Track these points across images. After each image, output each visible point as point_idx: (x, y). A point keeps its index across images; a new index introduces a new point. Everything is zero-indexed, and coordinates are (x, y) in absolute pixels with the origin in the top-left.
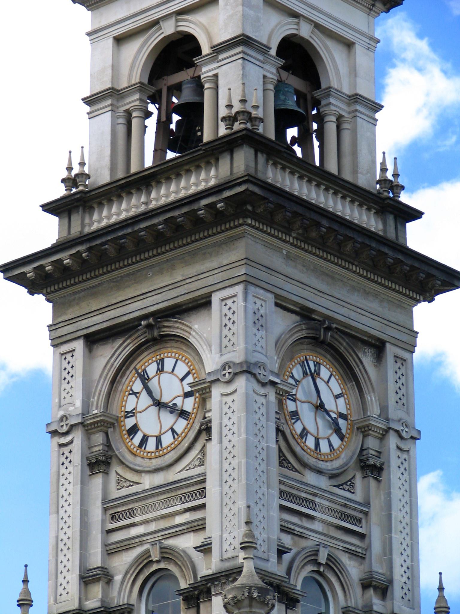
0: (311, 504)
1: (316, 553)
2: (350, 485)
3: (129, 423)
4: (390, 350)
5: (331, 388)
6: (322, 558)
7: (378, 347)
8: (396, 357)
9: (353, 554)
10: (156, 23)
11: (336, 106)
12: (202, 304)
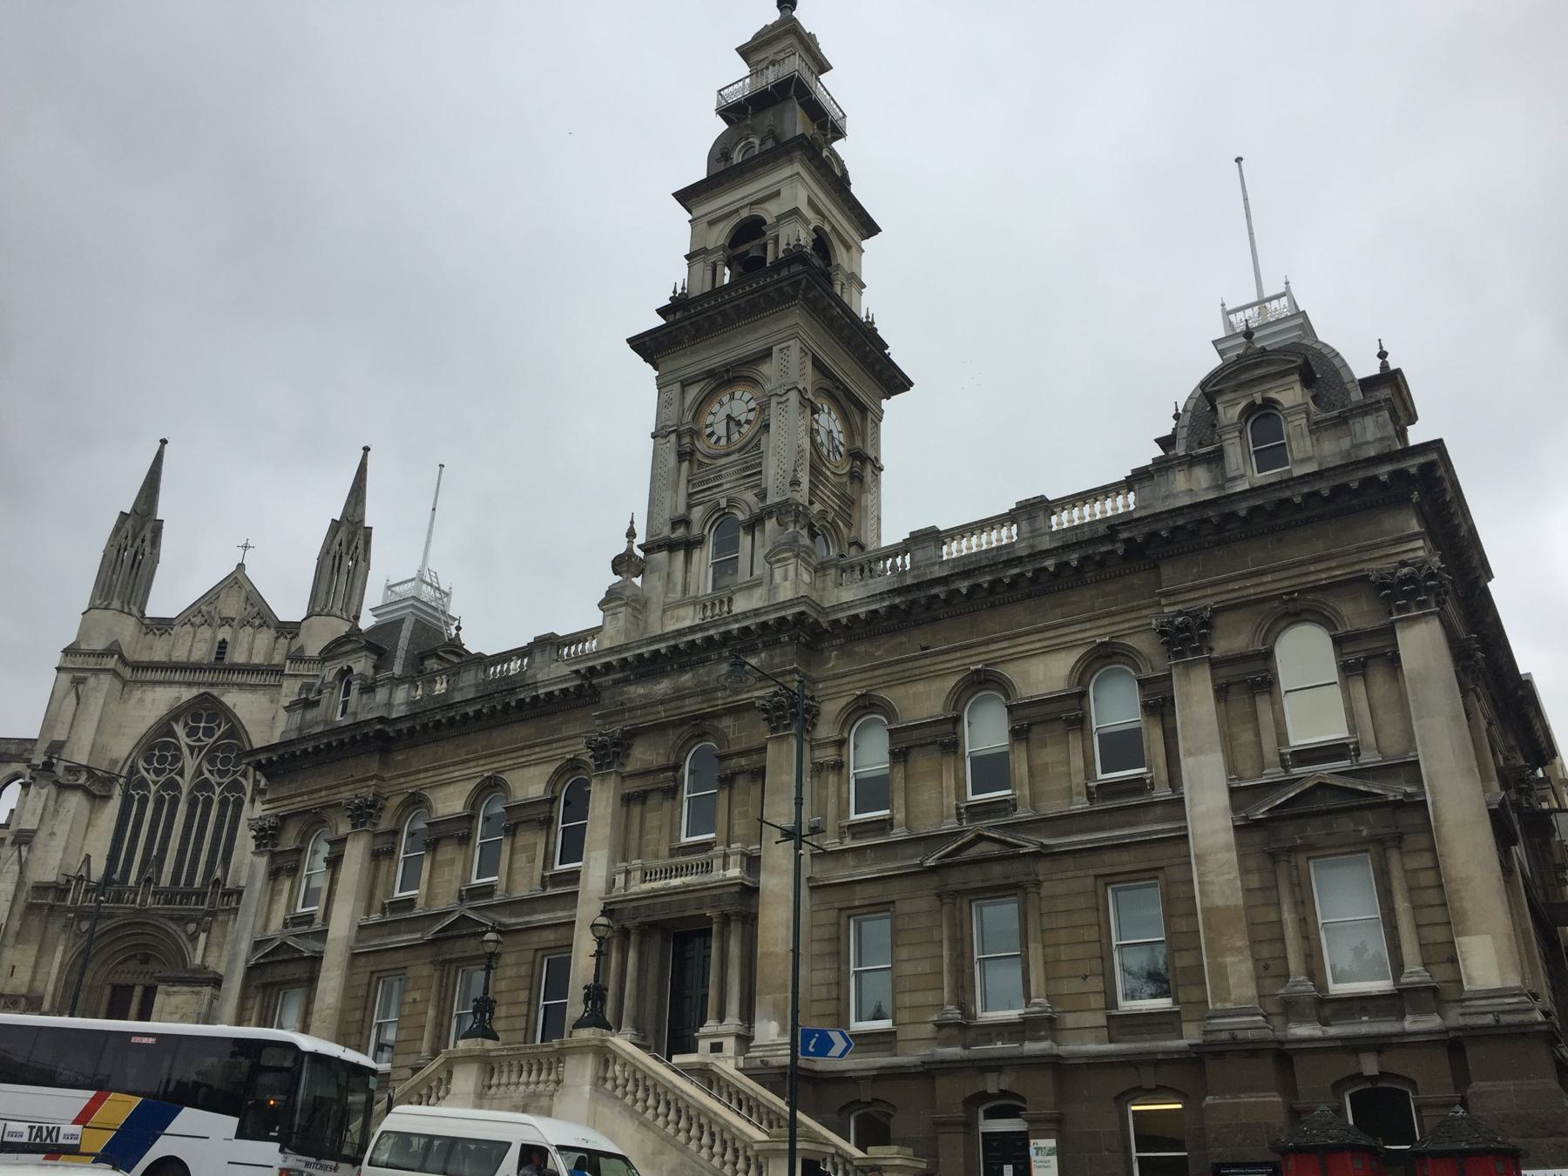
3: (709, 431)
10: (737, 211)
12: (766, 354)
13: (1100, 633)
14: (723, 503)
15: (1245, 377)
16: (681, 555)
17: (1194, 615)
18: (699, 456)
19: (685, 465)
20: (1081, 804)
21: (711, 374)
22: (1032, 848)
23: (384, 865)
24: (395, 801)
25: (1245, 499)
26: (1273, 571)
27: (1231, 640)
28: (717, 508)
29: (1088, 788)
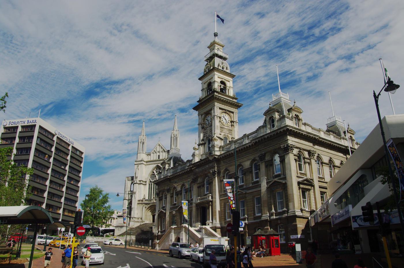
4: (234, 113)
9: (230, 134)
10: (208, 81)
11: (228, 88)
13: (252, 157)
14: (208, 136)
15: (269, 112)
16: (203, 146)
17: (262, 154)
18: (205, 128)
19: (203, 129)
20: (251, 185)
21: (205, 113)
22: (244, 193)
23: (172, 198)
24: (172, 188)
25: (266, 135)
26: (271, 146)
27: (267, 158)
28: (207, 137)
29: (252, 182)
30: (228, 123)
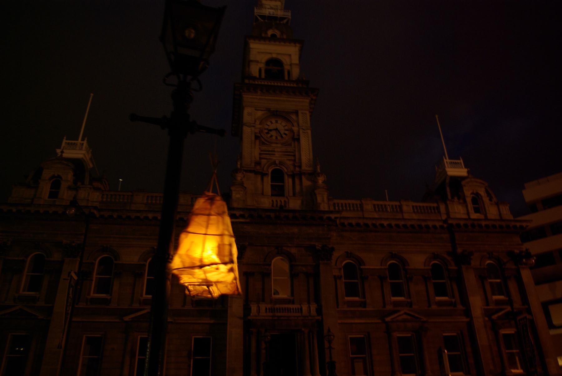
0: (274, 151)
1: (275, 162)
2: (290, 145)
4: (300, 112)
5: (281, 125)
6: (277, 162)
7: (297, 113)
8: (302, 113)
11: (287, 68)
30: (284, 136)
